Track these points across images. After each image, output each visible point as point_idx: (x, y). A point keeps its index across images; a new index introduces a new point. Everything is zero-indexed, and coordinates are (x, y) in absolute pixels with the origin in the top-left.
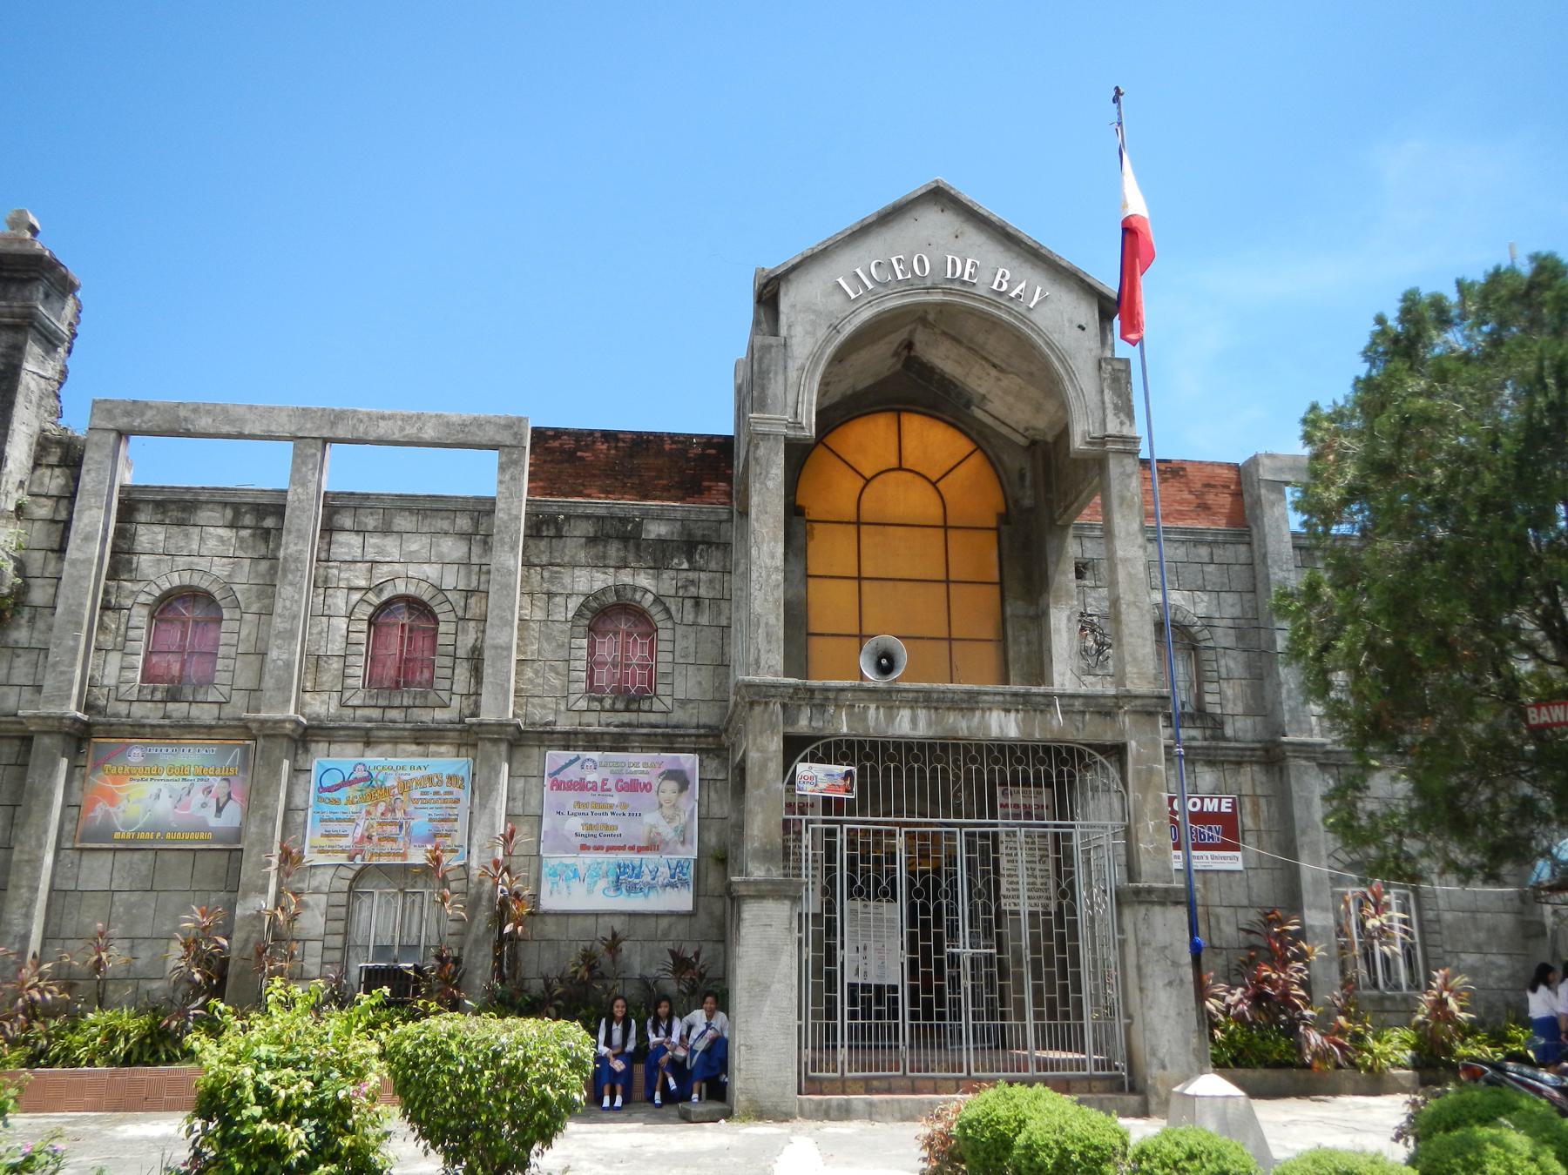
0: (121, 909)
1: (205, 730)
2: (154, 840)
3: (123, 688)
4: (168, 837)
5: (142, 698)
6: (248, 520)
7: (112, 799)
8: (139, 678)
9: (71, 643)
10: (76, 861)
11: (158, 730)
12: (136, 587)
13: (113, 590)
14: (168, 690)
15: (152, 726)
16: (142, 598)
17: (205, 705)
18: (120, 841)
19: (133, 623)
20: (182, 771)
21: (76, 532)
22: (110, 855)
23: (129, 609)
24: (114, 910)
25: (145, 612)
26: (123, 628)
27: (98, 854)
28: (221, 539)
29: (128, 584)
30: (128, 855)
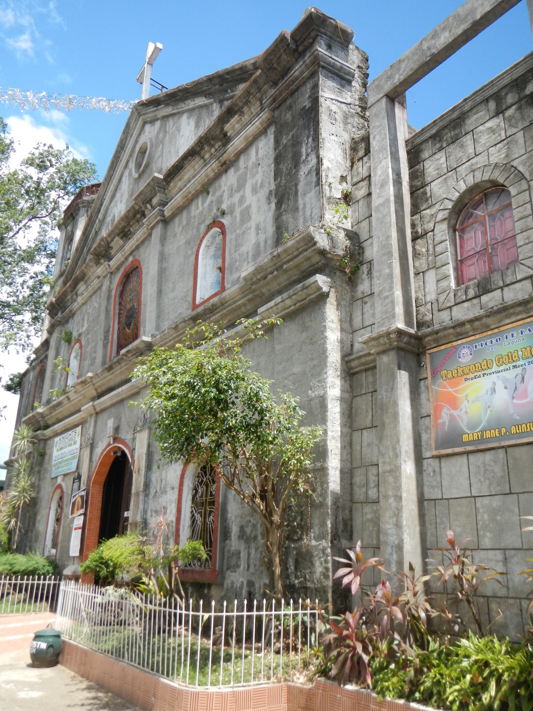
0: (486, 516)
1: (520, 309)
2: (501, 437)
3: (442, 298)
4: (513, 430)
5: (458, 301)
6: (510, 99)
7: (454, 403)
8: (453, 285)
9: (387, 271)
10: (437, 469)
11: (477, 324)
12: (433, 211)
13: (417, 222)
14: (478, 285)
15: (471, 321)
16: (440, 216)
17: (518, 286)
18: (469, 443)
19: (438, 239)
20: (511, 358)
21: (375, 185)
22: (463, 460)
23: (433, 231)
24: (479, 518)
25: (444, 226)
26: (431, 248)
27: (453, 460)
28: (492, 130)
29: (428, 211)
30: (480, 455)
